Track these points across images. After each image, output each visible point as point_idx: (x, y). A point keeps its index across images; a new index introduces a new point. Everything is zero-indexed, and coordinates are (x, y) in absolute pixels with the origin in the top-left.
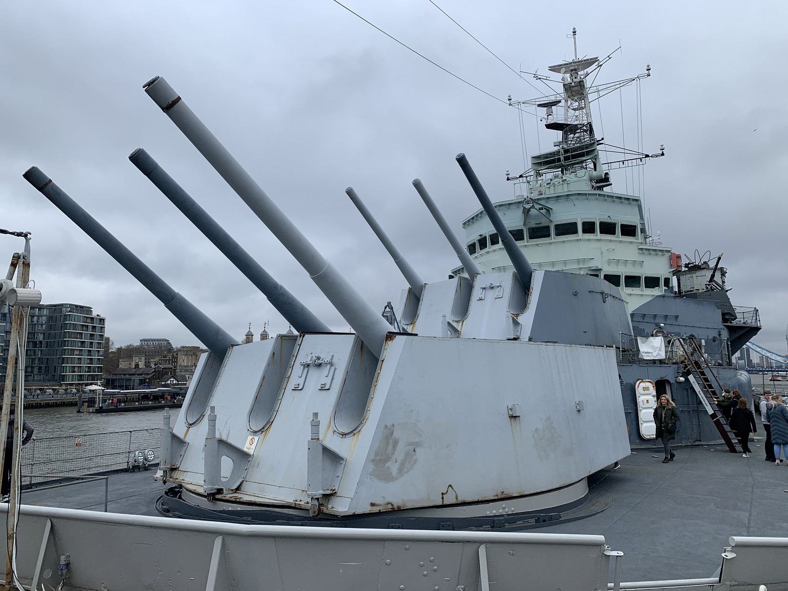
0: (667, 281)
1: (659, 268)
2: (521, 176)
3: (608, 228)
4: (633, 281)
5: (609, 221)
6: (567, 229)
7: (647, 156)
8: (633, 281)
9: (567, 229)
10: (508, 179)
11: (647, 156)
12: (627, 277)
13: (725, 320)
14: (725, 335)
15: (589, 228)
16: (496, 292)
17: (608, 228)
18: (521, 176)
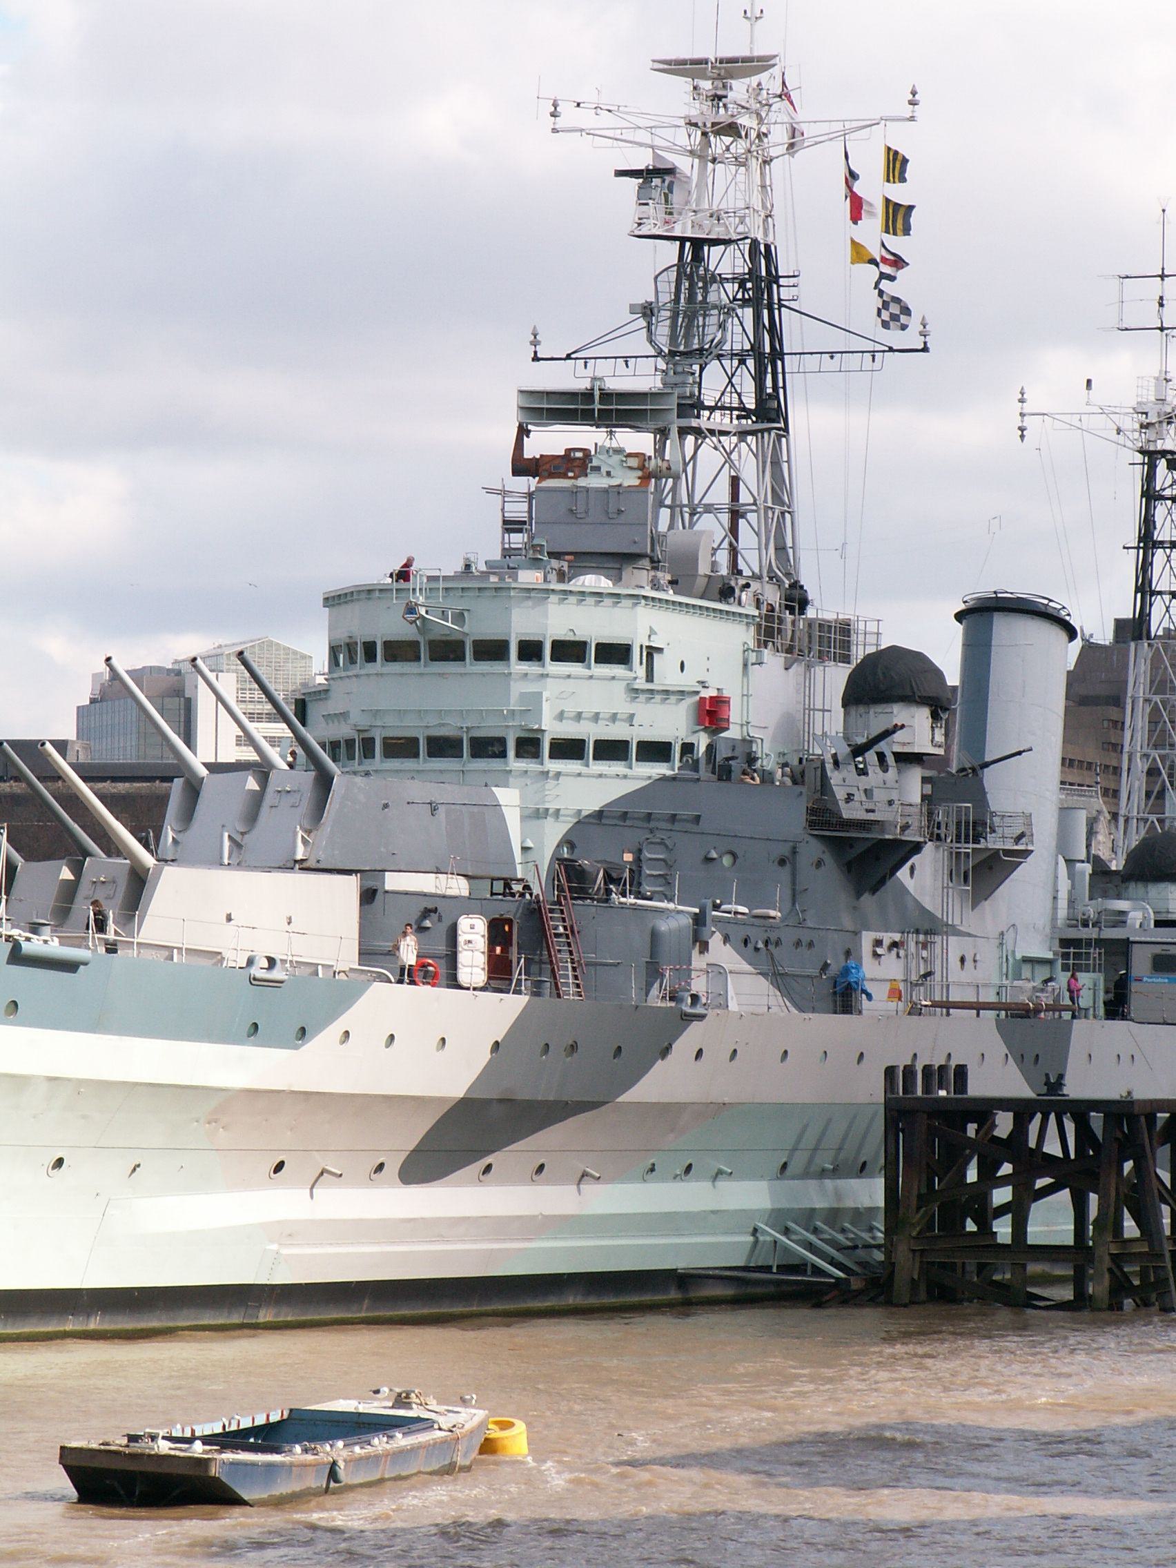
0: (688, 748)
1: (672, 723)
2: (568, 357)
3: (569, 651)
4: (611, 750)
5: (570, 637)
6: (493, 651)
7: (891, 350)
8: (611, 750)
9: (493, 651)
10: (536, 359)
11: (891, 350)
12: (598, 743)
13: (812, 824)
14: (812, 849)
15: (530, 651)
16: (292, 799)
17: (569, 651)
18: (568, 357)
